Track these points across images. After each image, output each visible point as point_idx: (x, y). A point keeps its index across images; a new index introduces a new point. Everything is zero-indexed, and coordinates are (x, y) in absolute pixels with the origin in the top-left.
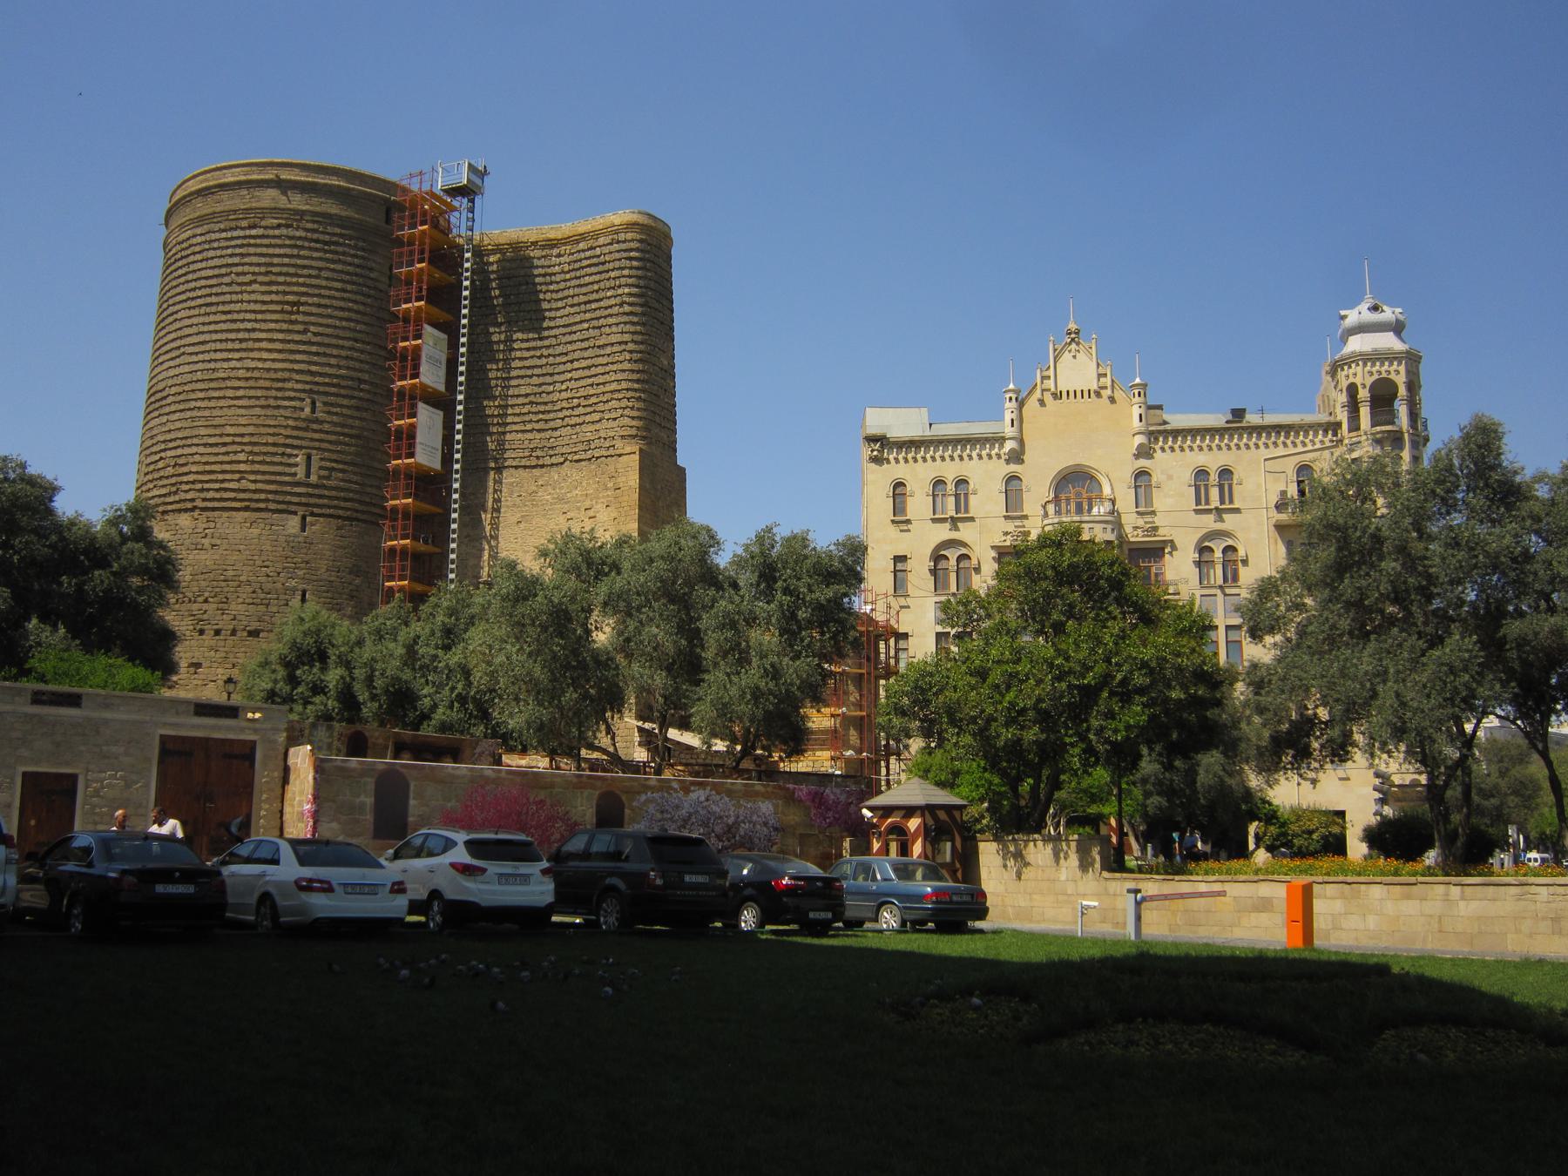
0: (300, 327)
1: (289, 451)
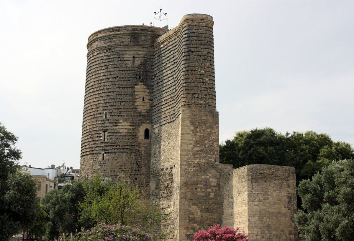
0: (102, 88)
1: (99, 132)
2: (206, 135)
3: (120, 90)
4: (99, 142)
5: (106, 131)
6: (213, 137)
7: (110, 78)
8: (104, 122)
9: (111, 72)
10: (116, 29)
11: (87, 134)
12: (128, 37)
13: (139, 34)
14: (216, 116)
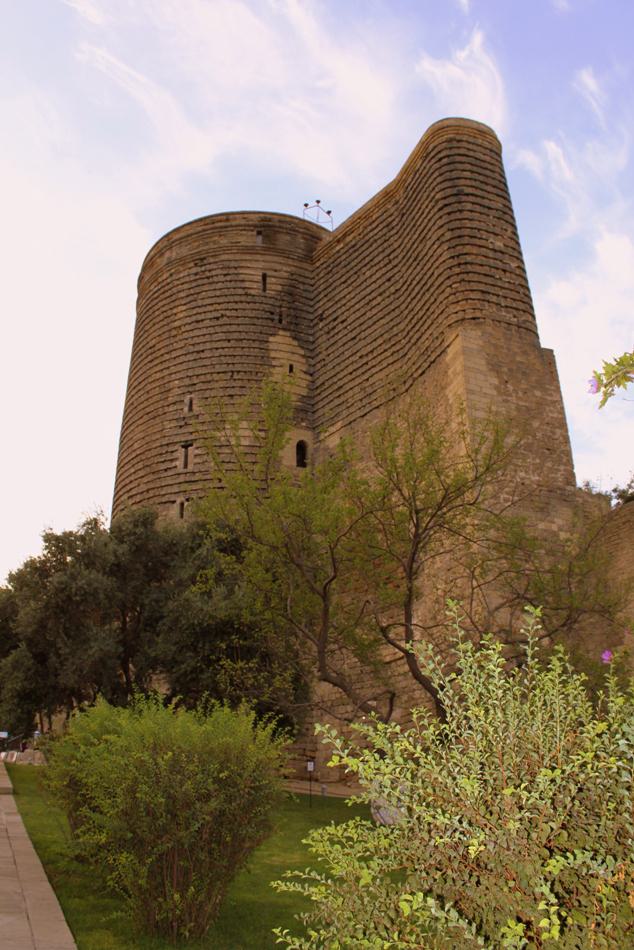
0: (182, 344)
1: (171, 449)
2: (534, 406)
3: (229, 345)
4: (170, 473)
5: (191, 445)
6: (551, 415)
7: (202, 320)
8: (186, 424)
9: (205, 306)
10: (219, 218)
11: (133, 462)
12: (250, 233)
13: (276, 229)
14: (548, 357)
